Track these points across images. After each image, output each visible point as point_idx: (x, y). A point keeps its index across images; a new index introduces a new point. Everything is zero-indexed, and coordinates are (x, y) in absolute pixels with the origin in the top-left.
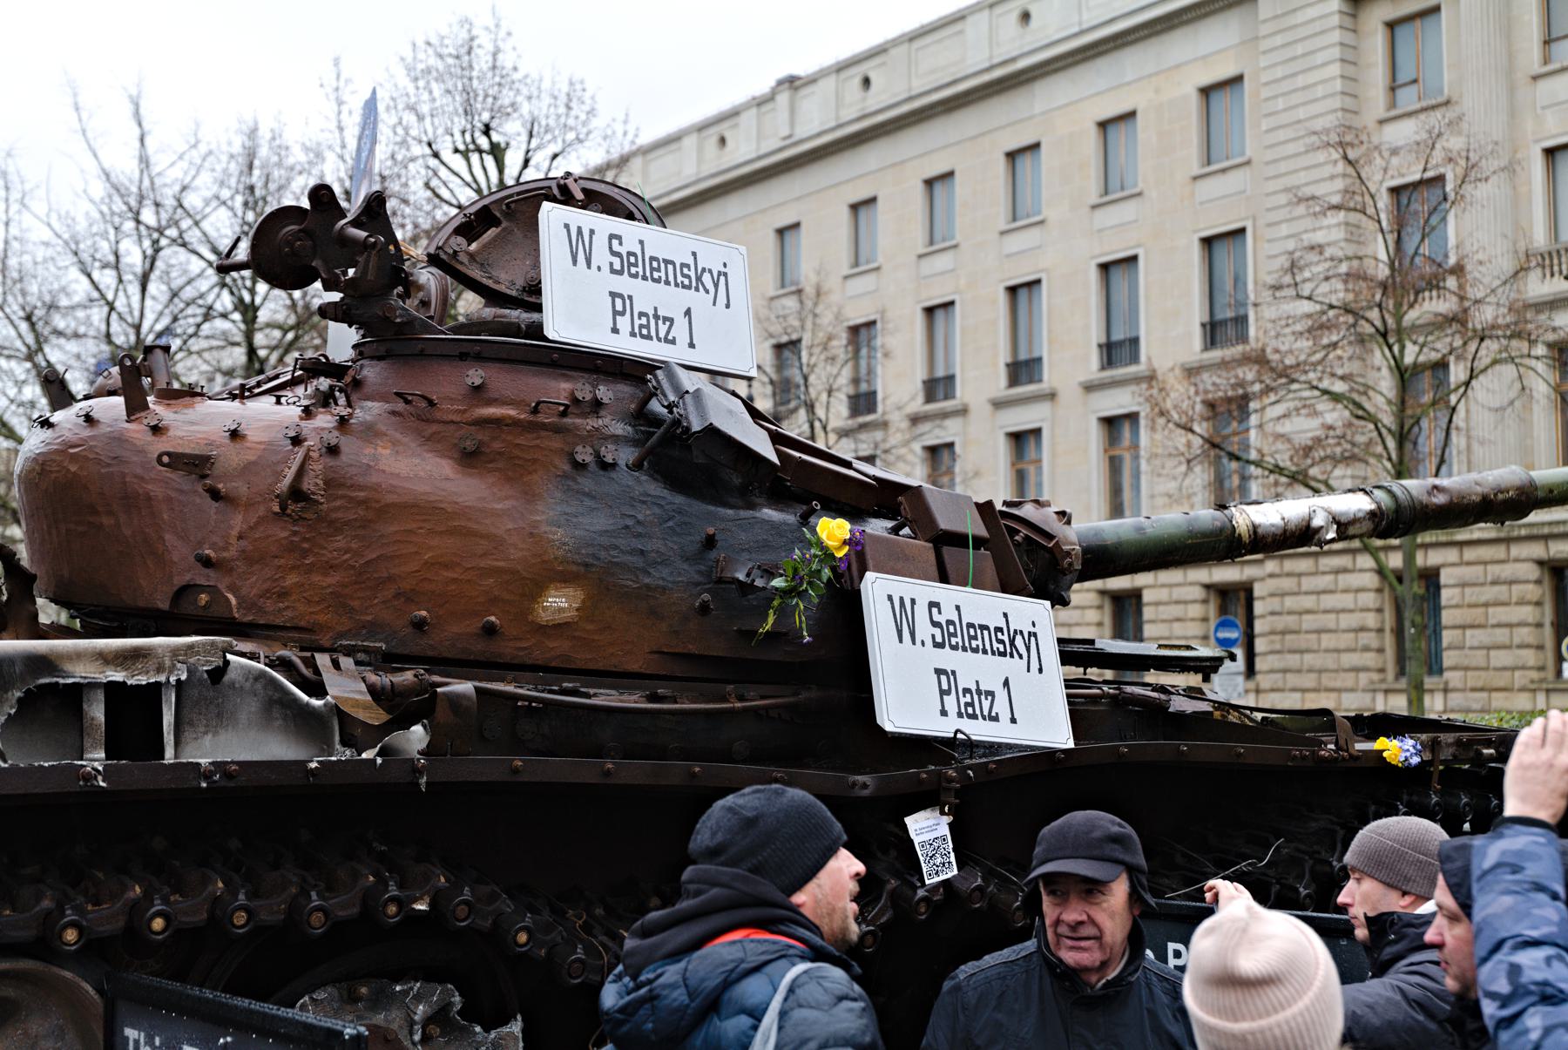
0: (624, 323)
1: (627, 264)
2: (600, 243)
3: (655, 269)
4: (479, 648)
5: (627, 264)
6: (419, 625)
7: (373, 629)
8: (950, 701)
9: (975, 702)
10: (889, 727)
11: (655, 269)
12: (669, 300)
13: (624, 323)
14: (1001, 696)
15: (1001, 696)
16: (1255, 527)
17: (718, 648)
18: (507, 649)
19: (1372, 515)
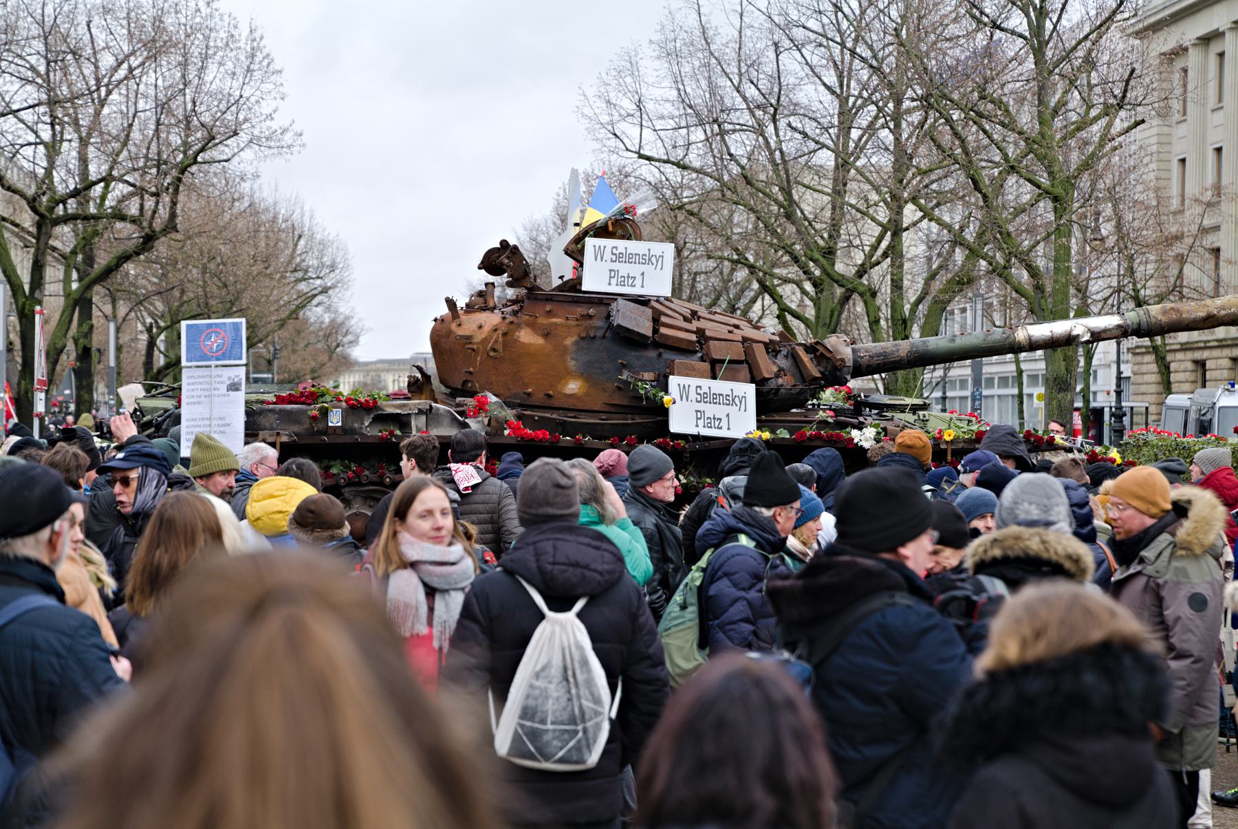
0: (614, 281)
1: (618, 257)
2: (608, 250)
3: (629, 258)
4: (547, 403)
5: (618, 257)
6: (529, 394)
7: (515, 395)
8: (701, 422)
9: (714, 421)
10: (672, 430)
11: (629, 258)
12: (634, 270)
13: (614, 281)
14: (725, 420)
15: (725, 420)
16: (1030, 337)
17: (625, 403)
18: (556, 403)
19: (1119, 326)
